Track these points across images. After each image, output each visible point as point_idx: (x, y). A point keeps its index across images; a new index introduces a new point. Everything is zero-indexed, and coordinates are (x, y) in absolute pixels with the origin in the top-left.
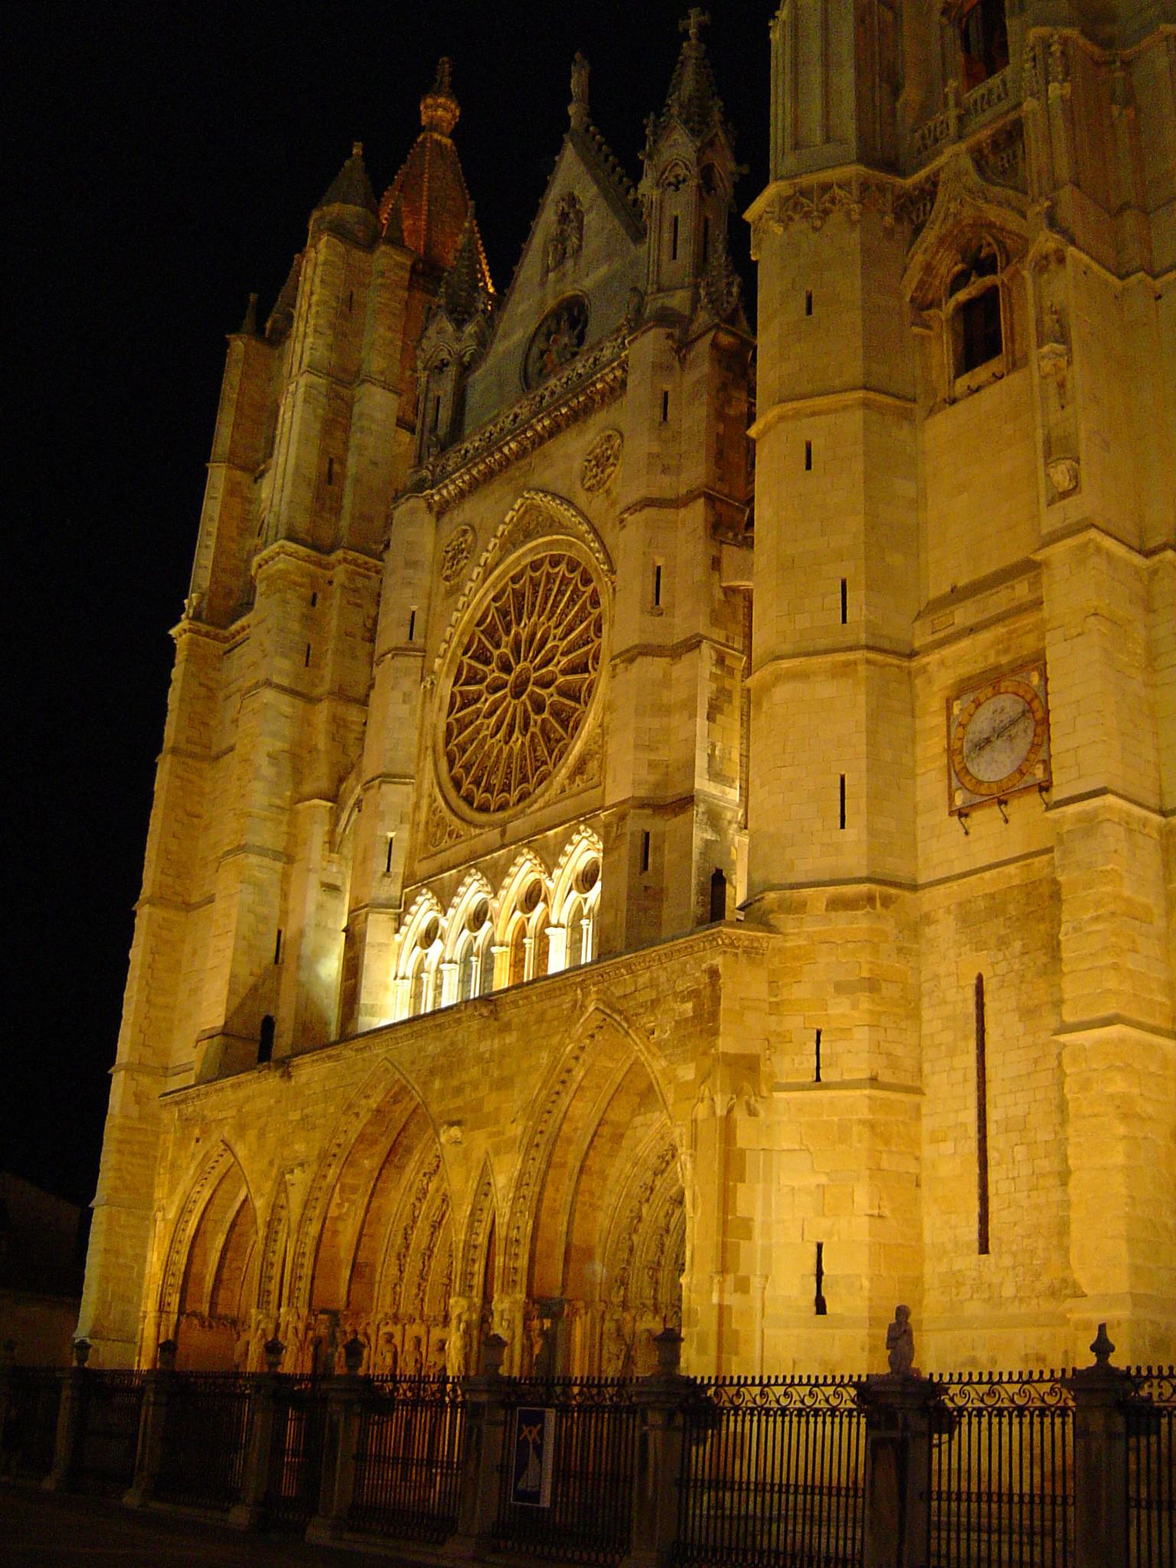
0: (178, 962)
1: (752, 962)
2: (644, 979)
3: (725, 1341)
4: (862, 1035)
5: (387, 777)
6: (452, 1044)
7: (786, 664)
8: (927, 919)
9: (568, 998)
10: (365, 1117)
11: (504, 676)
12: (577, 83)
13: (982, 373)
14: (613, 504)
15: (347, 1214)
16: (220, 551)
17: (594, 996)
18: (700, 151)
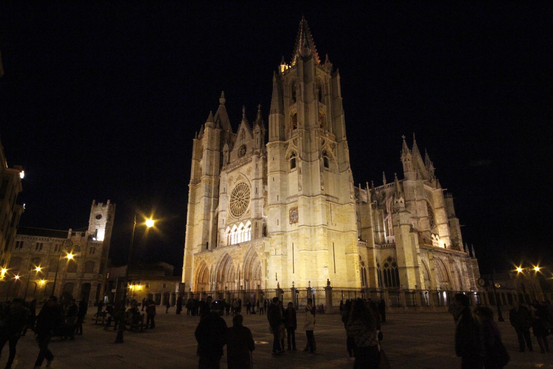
1: (268, 241)
2: (256, 243)
3: (266, 284)
4: (280, 249)
5: (222, 211)
7: (271, 206)
8: (287, 236)
10: (223, 257)
12: (244, 111)
13: (293, 169)
18: (260, 129)
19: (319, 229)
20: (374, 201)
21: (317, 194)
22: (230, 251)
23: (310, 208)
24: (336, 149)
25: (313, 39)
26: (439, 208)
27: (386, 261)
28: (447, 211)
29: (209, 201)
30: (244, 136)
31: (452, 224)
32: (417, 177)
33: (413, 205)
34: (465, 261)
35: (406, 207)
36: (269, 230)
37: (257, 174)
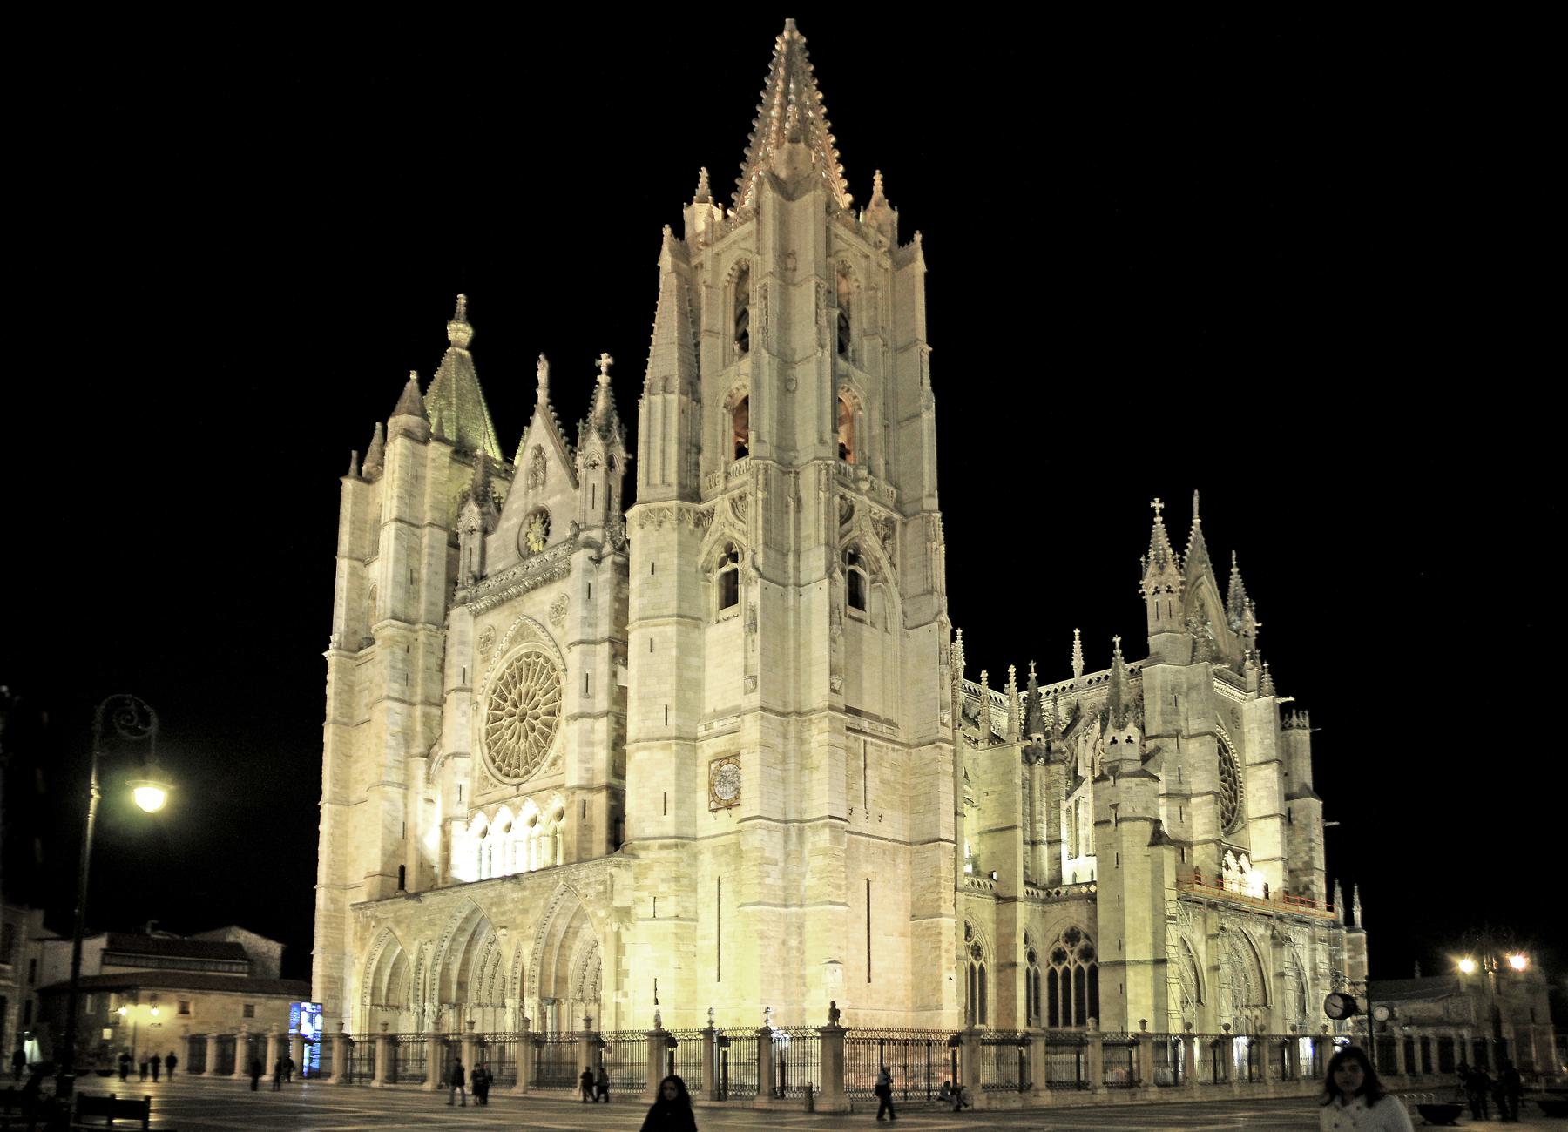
0: (347, 832)
1: (626, 869)
2: (583, 874)
3: (618, 1015)
4: (672, 899)
5: (456, 755)
6: (500, 893)
8: (700, 852)
16: (350, 609)
19: (815, 831)
20: (1035, 736)
23: (784, 759)
24: (898, 540)
25: (824, 110)
26: (1261, 763)
28: (1286, 775)
30: (541, 475)
31: (1299, 818)
33: (1172, 752)
34: (1324, 941)
35: (1145, 758)
36: (632, 829)
37: (589, 622)
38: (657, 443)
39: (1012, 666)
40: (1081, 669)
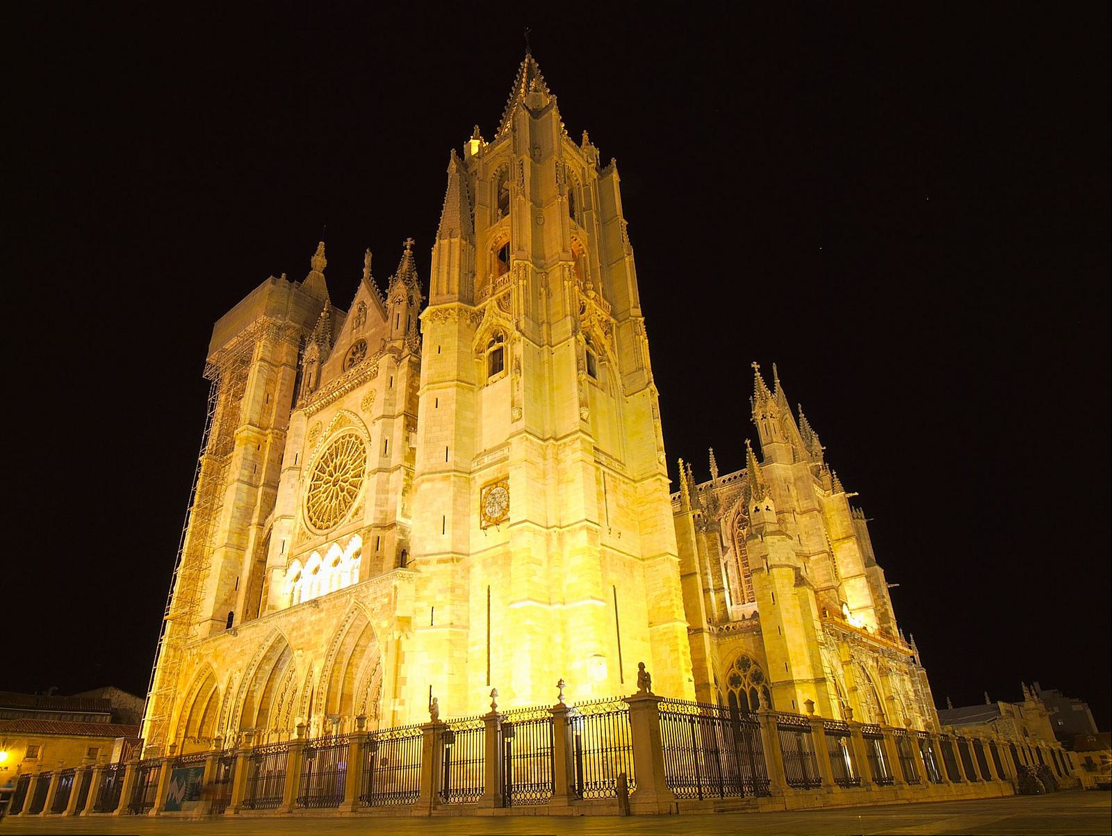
2: (371, 590)
4: (448, 608)
5: (283, 517)
6: (301, 618)
8: (472, 566)
9: (343, 599)
10: (266, 649)
11: (330, 478)
12: (367, 260)
13: (497, 376)
14: (372, 416)
15: (258, 689)
17: (354, 597)
21: (568, 433)
22: (291, 626)
23: (545, 475)
27: (735, 670)
29: (249, 494)
32: (794, 456)
33: (792, 523)
36: (413, 552)
37: (389, 402)
38: (445, 268)
39: (680, 459)
40: (716, 474)
